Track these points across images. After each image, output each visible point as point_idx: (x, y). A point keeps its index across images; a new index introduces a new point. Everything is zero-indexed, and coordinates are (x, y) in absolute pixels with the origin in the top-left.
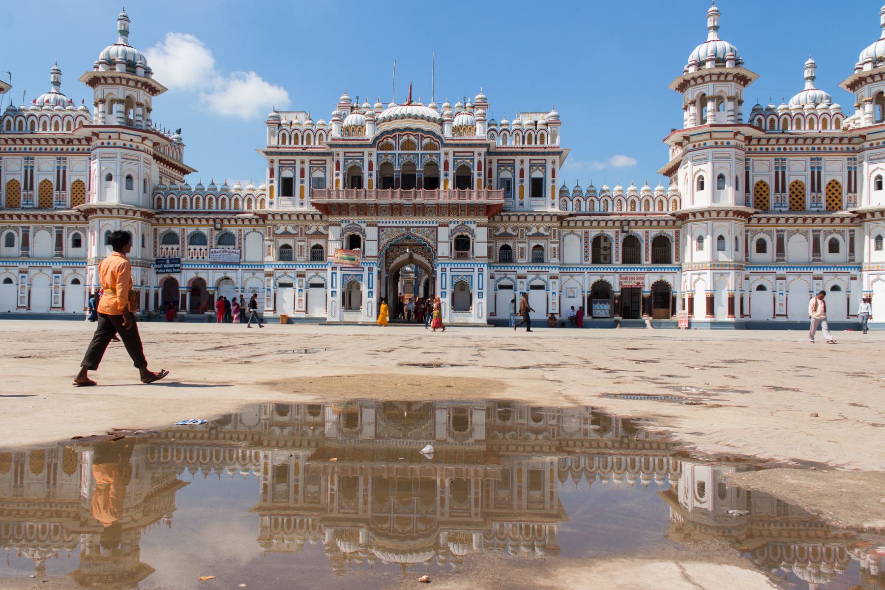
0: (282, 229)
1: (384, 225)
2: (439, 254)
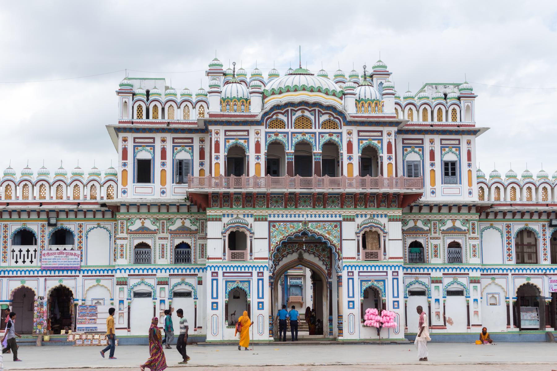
0: (137, 225)
1: (276, 219)
2: (345, 254)
